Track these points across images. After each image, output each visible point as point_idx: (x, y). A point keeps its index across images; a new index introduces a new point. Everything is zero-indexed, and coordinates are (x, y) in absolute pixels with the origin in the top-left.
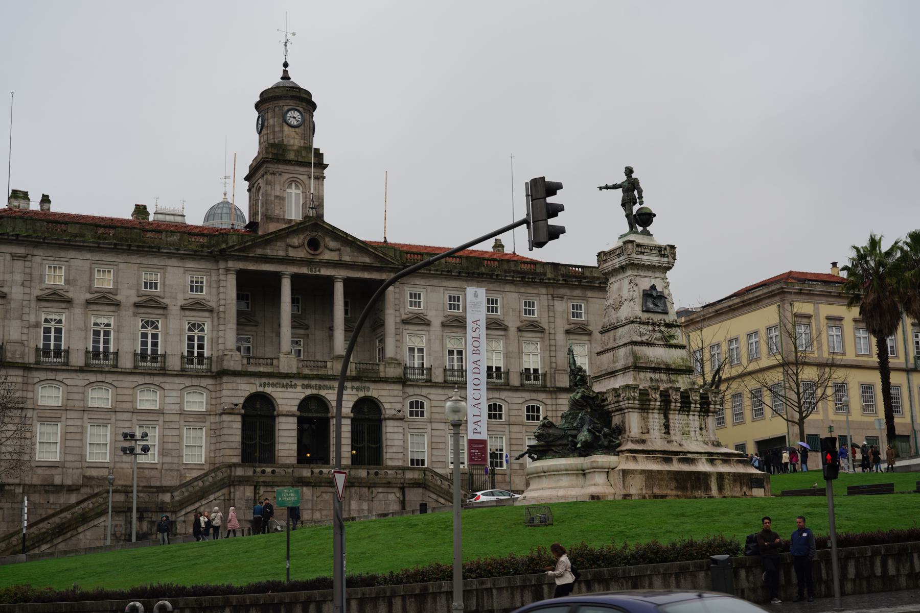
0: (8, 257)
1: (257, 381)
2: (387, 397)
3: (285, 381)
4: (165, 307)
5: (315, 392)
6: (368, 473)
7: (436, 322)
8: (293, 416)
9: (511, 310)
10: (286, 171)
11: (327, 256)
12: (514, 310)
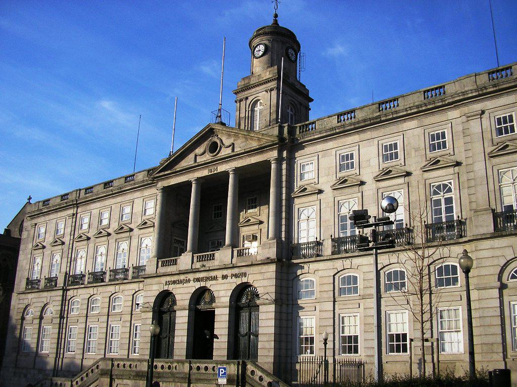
0: (67, 218)
1: (164, 280)
2: (262, 281)
3: (182, 277)
4: (131, 230)
5: (203, 284)
6: (191, 368)
7: (326, 187)
8: (184, 309)
9: (413, 151)
10: (249, 95)
11: (225, 152)
12: (417, 150)
